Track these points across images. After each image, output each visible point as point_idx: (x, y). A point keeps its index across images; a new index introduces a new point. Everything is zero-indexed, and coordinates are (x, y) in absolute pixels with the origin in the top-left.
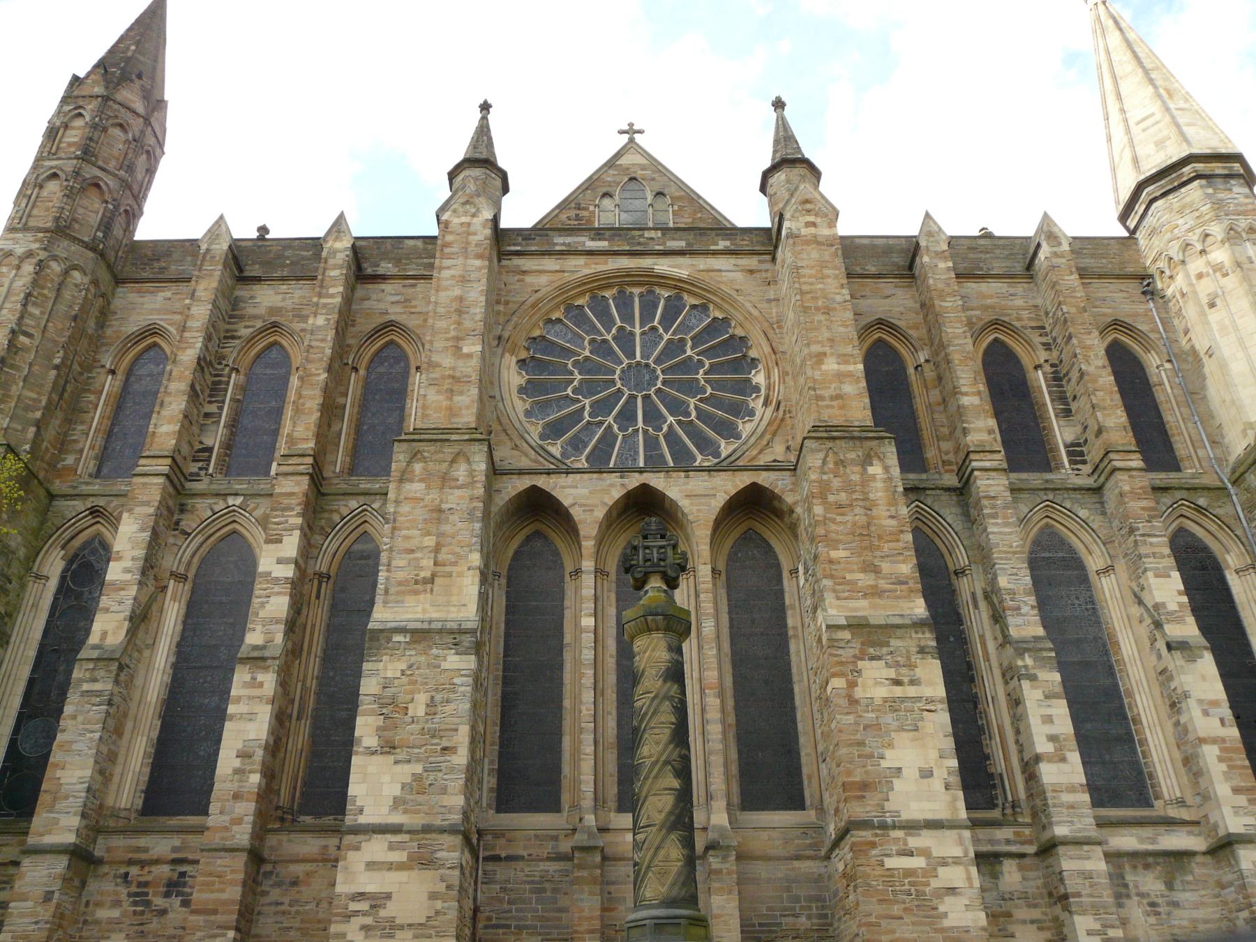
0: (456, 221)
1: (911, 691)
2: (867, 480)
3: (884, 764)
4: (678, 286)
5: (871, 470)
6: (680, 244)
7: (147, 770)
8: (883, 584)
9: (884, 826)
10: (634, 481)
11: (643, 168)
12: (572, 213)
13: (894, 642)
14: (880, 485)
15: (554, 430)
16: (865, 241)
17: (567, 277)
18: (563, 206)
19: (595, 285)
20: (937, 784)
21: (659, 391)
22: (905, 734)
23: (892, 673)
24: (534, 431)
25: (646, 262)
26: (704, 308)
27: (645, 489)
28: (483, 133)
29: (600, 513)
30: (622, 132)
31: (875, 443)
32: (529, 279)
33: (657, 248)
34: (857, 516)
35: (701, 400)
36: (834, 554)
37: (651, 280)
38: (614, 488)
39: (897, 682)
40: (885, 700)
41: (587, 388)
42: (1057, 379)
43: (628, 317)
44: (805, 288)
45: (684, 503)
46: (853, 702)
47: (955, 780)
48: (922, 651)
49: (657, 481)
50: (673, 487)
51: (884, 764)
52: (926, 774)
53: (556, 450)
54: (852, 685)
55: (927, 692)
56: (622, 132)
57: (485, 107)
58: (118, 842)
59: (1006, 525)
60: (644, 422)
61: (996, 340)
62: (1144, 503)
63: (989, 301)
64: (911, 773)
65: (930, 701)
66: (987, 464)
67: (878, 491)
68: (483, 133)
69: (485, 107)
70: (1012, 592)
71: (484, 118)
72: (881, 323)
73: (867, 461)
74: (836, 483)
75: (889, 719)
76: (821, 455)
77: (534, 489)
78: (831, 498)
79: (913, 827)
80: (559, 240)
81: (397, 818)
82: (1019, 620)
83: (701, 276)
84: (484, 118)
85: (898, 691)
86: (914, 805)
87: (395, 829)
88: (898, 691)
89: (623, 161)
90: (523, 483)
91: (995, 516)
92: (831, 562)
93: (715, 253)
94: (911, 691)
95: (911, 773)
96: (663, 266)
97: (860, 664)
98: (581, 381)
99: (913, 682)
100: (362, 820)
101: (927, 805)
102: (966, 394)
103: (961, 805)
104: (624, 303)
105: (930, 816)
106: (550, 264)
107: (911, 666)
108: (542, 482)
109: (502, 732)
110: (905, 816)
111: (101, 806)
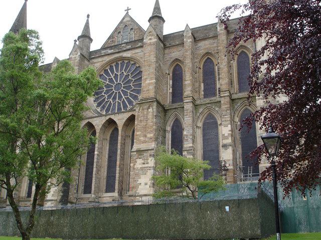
0: (73, 57)
1: (146, 165)
2: (148, 113)
3: (138, 182)
4: (129, 59)
5: (149, 110)
6: (129, 47)
7: (27, 189)
8: (147, 140)
9: (135, 196)
10: (108, 118)
11: (129, 21)
12: (111, 40)
13: (145, 154)
14: (151, 114)
15: (99, 105)
16: (177, 34)
17: (104, 62)
18: (109, 38)
19: (110, 63)
20: (148, 186)
21: (124, 87)
22: (143, 176)
23: (143, 162)
24: (95, 105)
25: (120, 54)
26: (135, 64)
27: (110, 119)
28: (87, 27)
29: (100, 127)
30: (125, 11)
31: (151, 103)
32: (96, 65)
33: (125, 49)
34: (143, 123)
35: (131, 91)
36: (138, 133)
37: (123, 59)
38: (103, 120)
39: (144, 164)
40: (141, 168)
41: (107, 92)
42: (219, 69)
43: (117, 71)
44: (146, 59)
45: (117, 122)
46: (134, 169)
47: (152, 185)
48: (150, 156)
49: (113, 117)
50: (115, 118)
51: (138, 182)
52: (146, 184)
53: (99, 110)
54: (134, 165)
55: (149, 165)
56: (125, 11)
57: (88, 16)
58: (23, 203)
59: (189, 117)
60: (118, 99)
61: (208, 58)
62: (226, 106)
63: (207, 46)
64: (143, 184)
65: (150, 167)
66: (188, 101)
67: (150, 116)
68: (87, 27)
69: (88, 16)
70: (187, 135)
71: (88, 20)
72: (177, 60)
73: (148, 108)
74: (141, 115)
75: (141, 172)
76: (139, 108)
77: (89, 122)
78: (140, 119)
79: (141, 196)
80: (103, 52)
81: (53, 198)
82: (187, 143)
83: (134, 55)
84: (88, 20)
85: (144, 166)
86: (142, 191)
87: (52, 200)
88: (144, 166)
89: (125, 20)
90: (86, 121)
91: (187, 115)
92: (137, 135)
93: (137, 48)
94: (146, 165)
95: (143, 184)
96: (125, 54)
97: (138, 160)
98: (106, 90)
99: (147, 163)
100: (47, 199)
101: (145, 191)
102: (187, 80)
103: (152, 190)
104: (117, 66)
105: (145, 193)
106: (100, 59)
107: (148, 159)
108: (90, 120)
109: (86, 177)
110: (140, 194)
111: (19, 197)
